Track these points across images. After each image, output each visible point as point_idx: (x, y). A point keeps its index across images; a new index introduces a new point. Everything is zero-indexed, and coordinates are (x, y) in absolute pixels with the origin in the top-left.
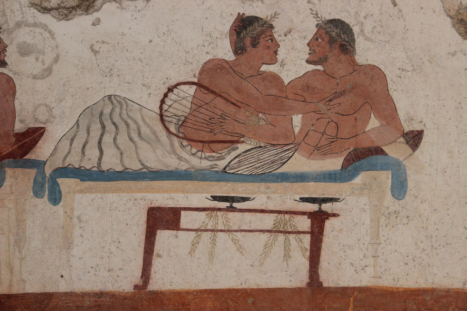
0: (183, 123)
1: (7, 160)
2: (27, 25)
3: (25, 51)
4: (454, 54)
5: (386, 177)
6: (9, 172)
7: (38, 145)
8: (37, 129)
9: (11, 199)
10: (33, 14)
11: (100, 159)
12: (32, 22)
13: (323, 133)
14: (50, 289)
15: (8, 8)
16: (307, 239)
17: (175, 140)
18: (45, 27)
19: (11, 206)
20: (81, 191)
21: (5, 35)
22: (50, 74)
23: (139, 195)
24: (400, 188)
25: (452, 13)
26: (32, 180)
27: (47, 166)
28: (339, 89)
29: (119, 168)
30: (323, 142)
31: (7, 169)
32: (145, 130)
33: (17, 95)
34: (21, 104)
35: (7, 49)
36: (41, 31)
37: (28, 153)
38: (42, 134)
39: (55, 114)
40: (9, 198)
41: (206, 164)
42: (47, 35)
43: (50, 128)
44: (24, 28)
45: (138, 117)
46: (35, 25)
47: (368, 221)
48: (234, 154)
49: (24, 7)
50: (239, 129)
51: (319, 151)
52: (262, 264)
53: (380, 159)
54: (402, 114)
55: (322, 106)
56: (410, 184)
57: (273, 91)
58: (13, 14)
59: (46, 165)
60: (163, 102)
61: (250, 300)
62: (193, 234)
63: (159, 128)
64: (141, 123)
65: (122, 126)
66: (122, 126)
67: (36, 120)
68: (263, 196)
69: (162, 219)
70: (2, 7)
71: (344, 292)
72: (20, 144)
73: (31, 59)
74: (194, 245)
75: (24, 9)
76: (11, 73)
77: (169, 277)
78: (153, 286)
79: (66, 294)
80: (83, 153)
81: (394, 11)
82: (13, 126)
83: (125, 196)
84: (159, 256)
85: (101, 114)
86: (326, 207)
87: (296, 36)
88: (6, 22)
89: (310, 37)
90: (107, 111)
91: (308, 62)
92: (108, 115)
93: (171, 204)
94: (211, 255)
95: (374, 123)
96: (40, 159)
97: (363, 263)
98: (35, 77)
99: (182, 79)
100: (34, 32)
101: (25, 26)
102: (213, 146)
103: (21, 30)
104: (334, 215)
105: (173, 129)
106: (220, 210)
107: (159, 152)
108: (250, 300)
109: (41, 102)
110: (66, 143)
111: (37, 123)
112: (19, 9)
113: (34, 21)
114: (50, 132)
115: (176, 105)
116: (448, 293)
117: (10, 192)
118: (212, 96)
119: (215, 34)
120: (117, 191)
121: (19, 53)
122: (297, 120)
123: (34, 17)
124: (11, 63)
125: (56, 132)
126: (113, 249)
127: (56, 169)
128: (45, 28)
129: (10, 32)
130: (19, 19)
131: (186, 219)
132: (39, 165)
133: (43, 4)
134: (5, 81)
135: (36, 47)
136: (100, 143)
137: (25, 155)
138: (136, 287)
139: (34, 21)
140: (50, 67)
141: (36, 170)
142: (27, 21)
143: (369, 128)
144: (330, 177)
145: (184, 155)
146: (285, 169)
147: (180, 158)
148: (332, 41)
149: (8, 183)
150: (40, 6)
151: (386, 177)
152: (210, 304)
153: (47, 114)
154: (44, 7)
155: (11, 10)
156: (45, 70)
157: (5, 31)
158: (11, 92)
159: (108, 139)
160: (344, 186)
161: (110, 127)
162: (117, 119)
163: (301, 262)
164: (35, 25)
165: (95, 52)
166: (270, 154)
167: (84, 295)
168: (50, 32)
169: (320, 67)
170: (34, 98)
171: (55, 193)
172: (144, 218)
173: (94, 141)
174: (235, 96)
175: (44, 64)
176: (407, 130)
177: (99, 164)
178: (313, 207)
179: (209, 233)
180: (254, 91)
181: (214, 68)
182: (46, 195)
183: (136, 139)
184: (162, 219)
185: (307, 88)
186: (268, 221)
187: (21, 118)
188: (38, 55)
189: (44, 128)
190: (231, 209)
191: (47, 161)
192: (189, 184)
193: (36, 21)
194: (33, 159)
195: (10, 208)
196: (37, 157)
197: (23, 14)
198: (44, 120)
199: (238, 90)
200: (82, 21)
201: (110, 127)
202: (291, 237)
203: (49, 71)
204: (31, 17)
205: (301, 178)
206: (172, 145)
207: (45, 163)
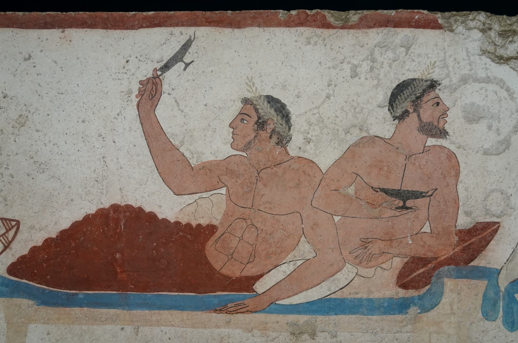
1: (446, 268)
3: (473, 116)
6: (449, 284)
7: (489, 247)
8: (487, 225)
9: (450, 322)
10: (486, 64)
12: (484, 75)
15: (451, 56)
18: (501, 83)
21: (446, 94)
22: (507, 148)
26: (481, 295)
27: (502, 276)
31: (446, 280)
33: (462, 177)
34: (466, 189)
35: (448, 112)
36: (497, 88)
37: (476, 258)
38: (496, 231)
39: (513, 204)
40: (448, 321)
42: (503, 94)
44: (473, 84)
46: (488, 80)
49: (473, 55)
58: (457, 65)
59: (500, 275)
67: (487, 212)
70: (442, 55)
72: (465, 245)
73: (481, 127)
75: (472, 58)
76: (453, 145)
82: (454, 220)
88: (448, 75)
96: (492, 267)
98: (486, 153)
100: (486, 90)
101: (474, 81)
103: (468, 86)
109: (494, 187)
111: (488, 217)
112: (466, 58)
113: (487, 74)
114: (507, 228)
117: (449, 312)
121: (465, 119)
123: (487, 69)
124: (454, 133)
127: (515, 281)
128: (502, 84)
129: (453, 89)
130: (466, 71)
132: (490, 275)
133: (498, 51)
134: (445, 157)
135: (488, 111)
137: (472, 260)
139: (487, 74)
140: (508, 138)
141: (486, 282)
142: (477, 74)
149: (447, 300)
150: (493, 53)
153: (503, 204)
154: (499, 55)
155: (455, 60)
156: (501, 143)
157: (445, 87)
158: (453, 173)
164: (488, 80)
168: (508, 90)
170: (484, 181)
171: (513, 314)
175: (499, 134)
182: (499, 316)
187: (466, 209)
188: (490, 121)
189: (498, 223)
191: (502, 269)
193: (489, 75)
194: (481, 267)
195: (449, 336)
196: (489, 263)
197: (470, 65)
198: (499, 212)
204: (483, 69)
207: (499, 272)
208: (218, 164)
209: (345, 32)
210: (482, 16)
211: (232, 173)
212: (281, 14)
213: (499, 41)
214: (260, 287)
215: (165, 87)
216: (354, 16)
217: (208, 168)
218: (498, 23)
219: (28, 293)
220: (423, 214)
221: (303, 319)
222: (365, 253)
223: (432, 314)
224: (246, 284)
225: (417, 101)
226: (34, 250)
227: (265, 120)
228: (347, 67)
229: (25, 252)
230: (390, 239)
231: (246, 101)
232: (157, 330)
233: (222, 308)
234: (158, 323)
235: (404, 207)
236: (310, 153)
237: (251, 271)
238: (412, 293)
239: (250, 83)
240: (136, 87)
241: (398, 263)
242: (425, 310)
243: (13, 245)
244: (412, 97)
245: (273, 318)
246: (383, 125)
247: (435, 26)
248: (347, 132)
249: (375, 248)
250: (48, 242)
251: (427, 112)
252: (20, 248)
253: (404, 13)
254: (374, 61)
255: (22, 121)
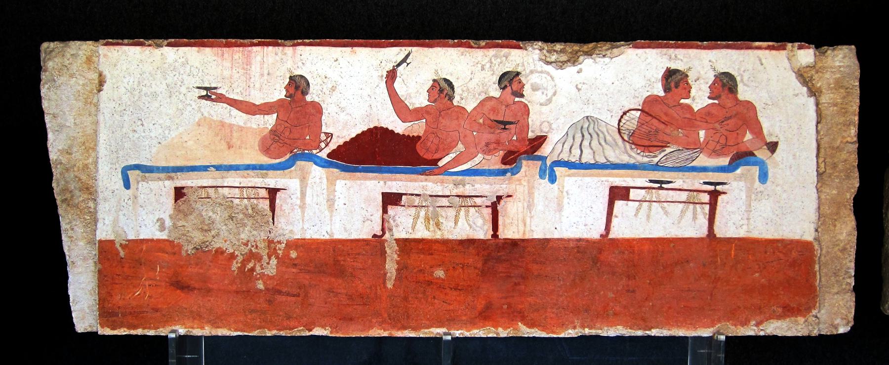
0: (632, 135)
2: (537, 72)
3: (535, 88)
4: (797, 95)
5: (755, 170)
6: (524, 162)
11: (581, 156)
13: (718, 142)
14: (548, 237)
16: (707, 207)
17: (628, 145)
18: (548, 74)
19: (525, 184)
20: (569, 176)
23: (604, 179)
24: (764, 177)
25: (796, 70)
28: (728, 115)
29: (592, 162)
30: (718, 148)
32: (608, 138)
41: (646, 160)
42: (549, 78)
43: (550, 136)
45: (604, 130)
46: (541, 72)
47: (744, 197)
48: (663, 154)
50: (667, 139)
51: (715, 153)
52: (679, 223)
53: (752, 159)
54: (765, 131)
55: (717, 126)
56: (770, 174)
57: (688, 116)
60: (620, 121)
61: (672, 245)
62: (637, 203)
63: (617, 137)
64: (606, 134)
65: (595, 136)
66: (595, 136)
67: (541, 131)
68: (680, 180)
69: (618, 194)
71: (729, 241)
73: (539, 93)
74: (638, 210)
77: (622, 229)
78: (611, 236)
79: (558, 239)
80: (570, 151)
81: (761, 68)
83: (596, 179)
84: (616, 217)
85: (582, 128)
86: (719, 188)
87: (702, 81)
89: (710, 83)
90: (586, 126)
91: (709, 98)
92: (586, 128)
93: (624, 184)
94: (648, 217)
95: (748, 136)
97: (741, 223)
98: (541, 104)
99: (632, 107)
102: (651, 149)
104: (724, 193)
105: (626, 138)
106: (654, 188)
107: (617, 152)
108: (672, 245)
110: (560, 146)
115: (628, 123)
116: (792, 242)
118: (650, 118)
119: (653, 80)
120: (591, 175)
122: (702, 133)
125: (553, 138)
126: (588, 212)
129: (527, 76)
130: (532, 68)
131: (633, 194)
132: (543, 159)
136: (581, 145)
138: (601, 236)
143: (745, 139)
144: (722, 169)
145: (633, 154)
146: (694, 164)
147: (630, 156)
148: (724, 85)
151: (755, 170)
152: (647, 247)
159: (586, 143)
160: (730, 174)
161: (587, 136)
162: (591, 131)
163: (703, 222)
164: (541, 72)
165: (579, 90)
166: (686, 154)
167: (569, 240)
169: (716, 101)
172: (607, 192)
173: (577, 144)
174: (664, 118)
176: (768, 141)
177: (580, 159)
178: (711, 188)
179: (647, 203)
180: (676, 115)
181: (652, 101)
183: (603, 143)
184: (618, 194)
185: (709, 114)
186: (684, 196)
190: (661, 188)
192: (636, 172)
199: (666, 114)
200: (571, 70)
201: (587, 136)
202: (698, 206)
203: (549, 101)
205: (704, 169)
206: (625, 148)
208: (422, 108)
209: (478, 50)
210: (540, 43)
211: (428, 113)
212: (451, 41)
213: (547, 54)
214: (441, 163)
215: (398, 74)
216: (483, 43)
217: (417, 110)
218: (546, 46)
219: (337, 166)
220: (513, 131)
221: (460, 178)
222: (488, 150)
223: (517, 176)
224: (435, 162)
225: (511, 81)
226: (339, 146)
227: (442, 89)
228: (480, 66)
229: (335, 147)
230: (498, 143)
231: (434, 81)
232: (394, 183)
233: (423, 173)
234: (395, 180)
235: (505, 129)
236: (463, 104)
237: (436, 156)
238: (508, 167)
239: (436, 72)
240: (385, 74)
241: (502, 153)
242: (513, 174)
243: (330, 144)
244: (510, 80)
245: (446, 177)
246: (496, 92)
247: (519, 48)
248: (479, 95)
249: (492, 146)
250: (346, 143)
251: (515, 86)
252: (333, 146)
253: (505, 42)
254: (491, 63)
255: (333, 89)
